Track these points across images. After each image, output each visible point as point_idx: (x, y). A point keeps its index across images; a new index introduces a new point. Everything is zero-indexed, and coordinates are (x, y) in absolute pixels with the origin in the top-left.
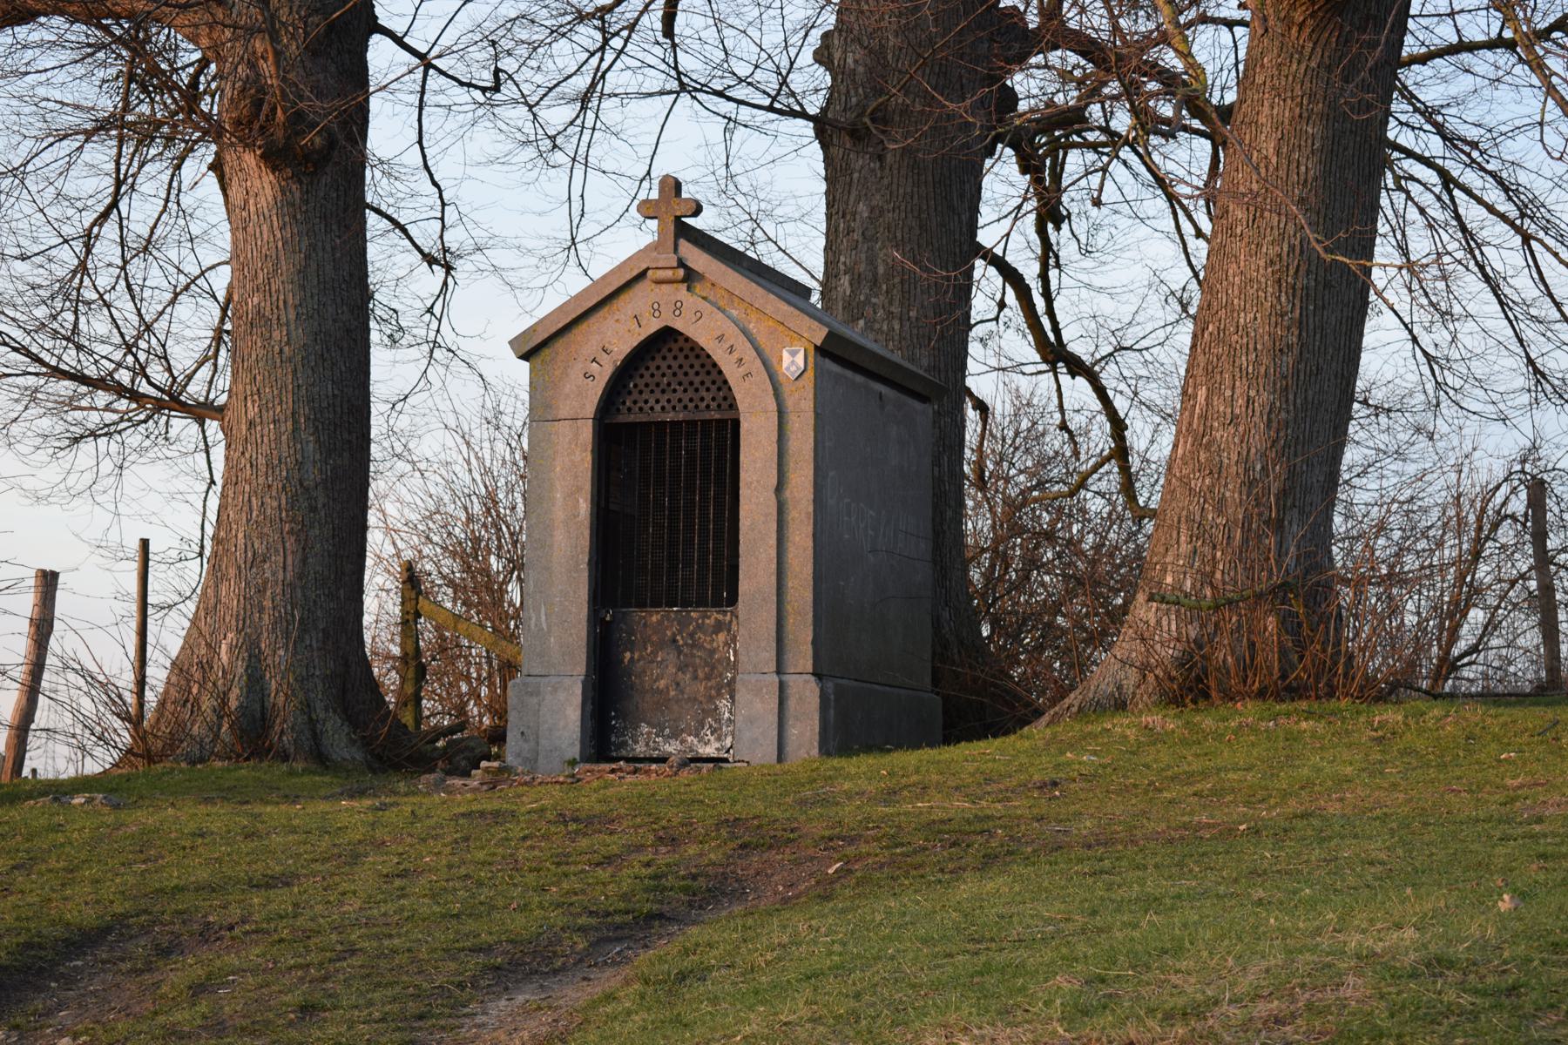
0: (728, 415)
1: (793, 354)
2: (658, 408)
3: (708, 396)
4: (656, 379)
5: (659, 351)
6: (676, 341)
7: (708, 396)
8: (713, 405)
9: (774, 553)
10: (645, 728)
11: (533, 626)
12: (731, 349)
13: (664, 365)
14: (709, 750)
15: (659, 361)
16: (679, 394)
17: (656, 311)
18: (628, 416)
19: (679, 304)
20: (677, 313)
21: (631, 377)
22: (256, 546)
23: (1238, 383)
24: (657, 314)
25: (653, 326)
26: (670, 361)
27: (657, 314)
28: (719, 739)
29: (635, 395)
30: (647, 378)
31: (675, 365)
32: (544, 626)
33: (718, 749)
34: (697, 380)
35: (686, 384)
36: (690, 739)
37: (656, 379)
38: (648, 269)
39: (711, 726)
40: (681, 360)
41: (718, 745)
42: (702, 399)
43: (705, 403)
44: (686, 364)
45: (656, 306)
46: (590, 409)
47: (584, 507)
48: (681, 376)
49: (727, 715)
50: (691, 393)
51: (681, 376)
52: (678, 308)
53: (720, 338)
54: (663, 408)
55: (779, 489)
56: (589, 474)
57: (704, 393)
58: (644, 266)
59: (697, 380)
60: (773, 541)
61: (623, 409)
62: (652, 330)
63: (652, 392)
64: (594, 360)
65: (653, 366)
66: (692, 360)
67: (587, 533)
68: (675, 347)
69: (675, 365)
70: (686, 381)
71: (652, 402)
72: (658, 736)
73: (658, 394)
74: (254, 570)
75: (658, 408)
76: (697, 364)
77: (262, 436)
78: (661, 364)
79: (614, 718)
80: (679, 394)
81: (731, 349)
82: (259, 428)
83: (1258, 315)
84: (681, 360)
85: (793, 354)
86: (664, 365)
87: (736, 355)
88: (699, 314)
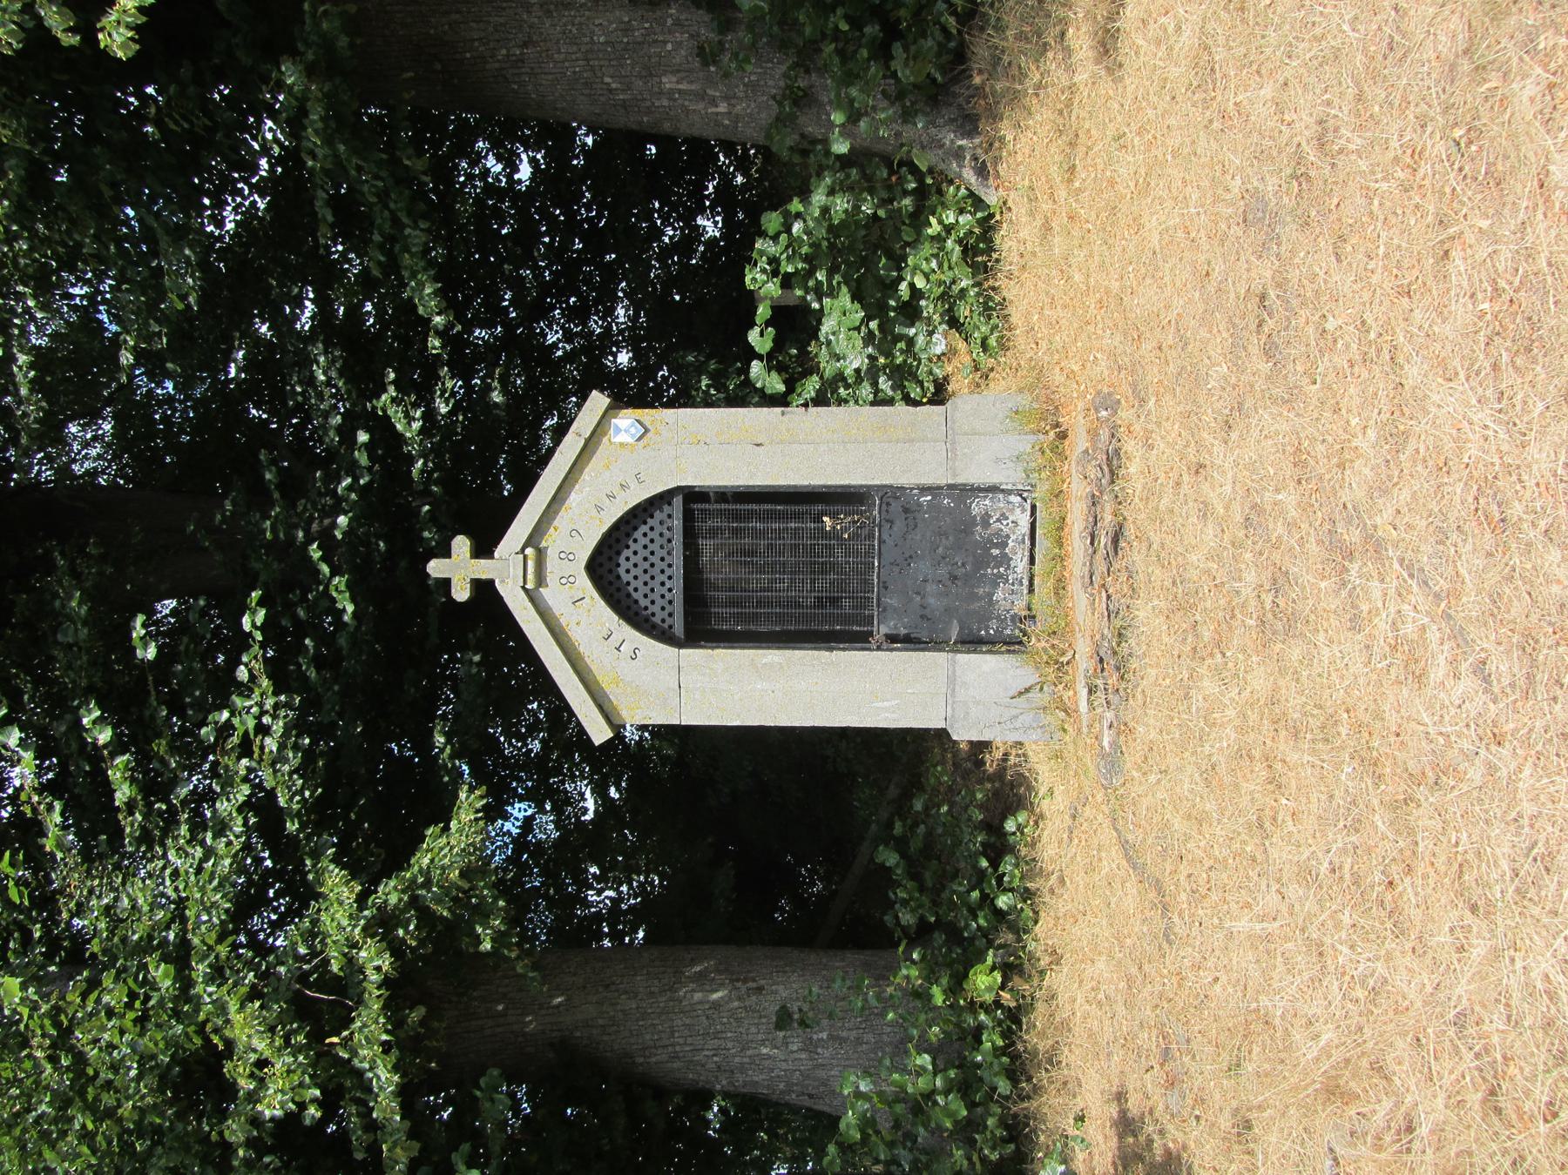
0: (678, 501)
1: (618, 430)
3: (658, 529)
5: (611, 583)
6: (601, 565)
10: (999, 595)
11: (895, 716)
12: (611, 497)
14: (1024, 521)
17: (567, 580)
18: (679, 630)
19: (562, 555)
20: (571, 557)
21: (637, 614)
22: (795, 1048)
23: (661, 38)
24: (572, 580)
27: (572, 580)
28: (1012, 511)
33: (1023, 511)
35: (646, 553)
36: (1011, 543)
38: (523, 588)
39: (998, 520)
41: (1018, 511)
42: (661, 535)
43: (665, 531)
45: (564, 581)
46: (669, 651)
49: (987, 502)
52: (566, 556)
53: (599, 509)
54: (670, 578)
56: (738, 651)
58: (522, 593)
61: (669, 621)
63: (652, 590)
64: (618, 649)
67: (798, 653)
72: (1007, 580)
73: (655, 584)
74: (819, 1050)
77: (685, 1044)
79: (987, 632)
81: (611, 497)
82: (678, 1048)
83: (597, 22)
85: (618, 430)
88: (574, 533)
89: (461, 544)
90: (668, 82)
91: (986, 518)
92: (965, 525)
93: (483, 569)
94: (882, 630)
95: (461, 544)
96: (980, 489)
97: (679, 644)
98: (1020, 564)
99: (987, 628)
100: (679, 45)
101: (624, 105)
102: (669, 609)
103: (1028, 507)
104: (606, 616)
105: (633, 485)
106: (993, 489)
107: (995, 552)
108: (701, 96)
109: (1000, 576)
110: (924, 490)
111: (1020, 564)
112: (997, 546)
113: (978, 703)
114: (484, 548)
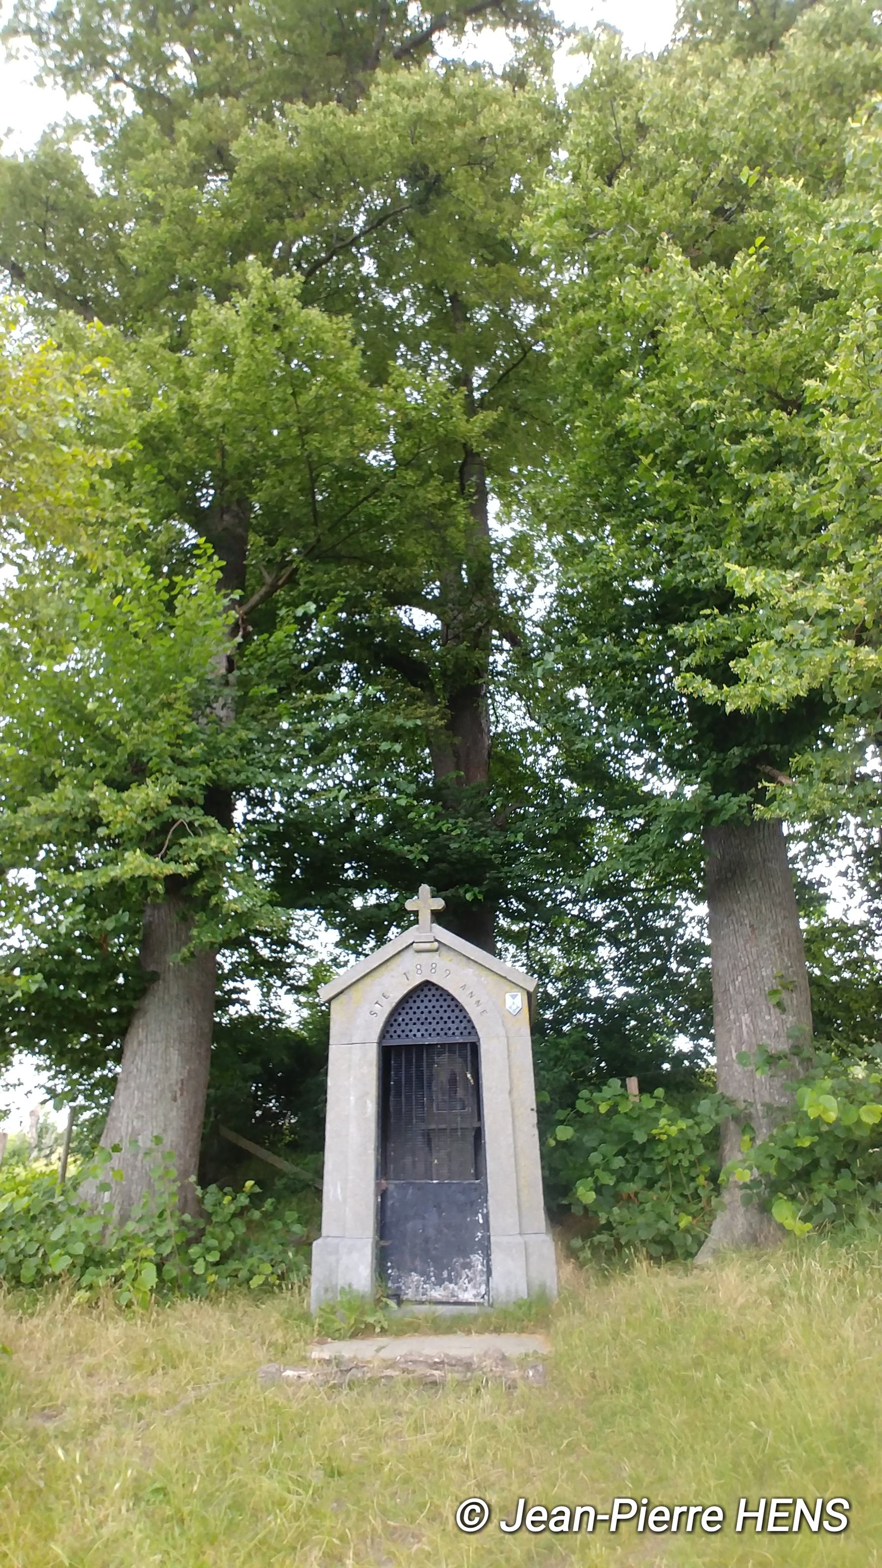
0: (471, 1039)
1: (514, 997)
2: (419, 1034)
3: (453, 1026)
4: (418, 1015)
7: (453, 1026)
8: (457, 1033)
9: (511, 1140)
10: (415, 1277)
13: (422, 1006)
15: (418, 1003)
16: (434, 1025)
17: (419, 970)
25: (417, 980)
26: (426, 1003)
28: (474, 1287)
29: (403, 1026)
30: (411, 1015)
31: (430, 1005)
32: (340, 1197)
34: (445, 1016)
36: (452, 1286)
37: (418, 1015)
40: (434, 1003)
44: (438, 1005)
47: (371, 1107)
48: (434, 1014)
50: (441, 1025)
51: (434, 1014)
53: (464, 987)
55: (510, 1092)
57: (450, 1024)
59: (445, 1016)
60: (510, 1131)
62: (417, 983)
65: (415, 1006)
66: (441, 1002)
68: (430, 994)
69: (430, 1005)
70: (438, 1016)
71: (415, 1031)
75: (419, 1034)
76: (445, 1004)
78: (423, 1005)
80: (434, 1025)
84: (434, 1003)
85: (514, 997)
86: (422, 1006)
87: (475, 999)
89: (439, 904)
90: (745, 1018)
91: (468, 1266)
92: (464, 1250)
93: (425, 917)
94: (391, 1186)
95: (439, 904)
96: (489, 1261)
97: (379, 1043)
98: (437, 1293)
99: (392, 1267)
100: (769, 1023)
101: (727, 990)
102: (403, 1035)
103: (479, 1300)
104: (397, 995)
105: (480, 1009)
106: (489, 1273)
107: (445, 1274)
108: (740, 1041)
109: (429, 1278)
110: (486, 1217)
111: (437, 1293)
112: (449, 1274)
113: (338, 1261)
114: (438, 917)
